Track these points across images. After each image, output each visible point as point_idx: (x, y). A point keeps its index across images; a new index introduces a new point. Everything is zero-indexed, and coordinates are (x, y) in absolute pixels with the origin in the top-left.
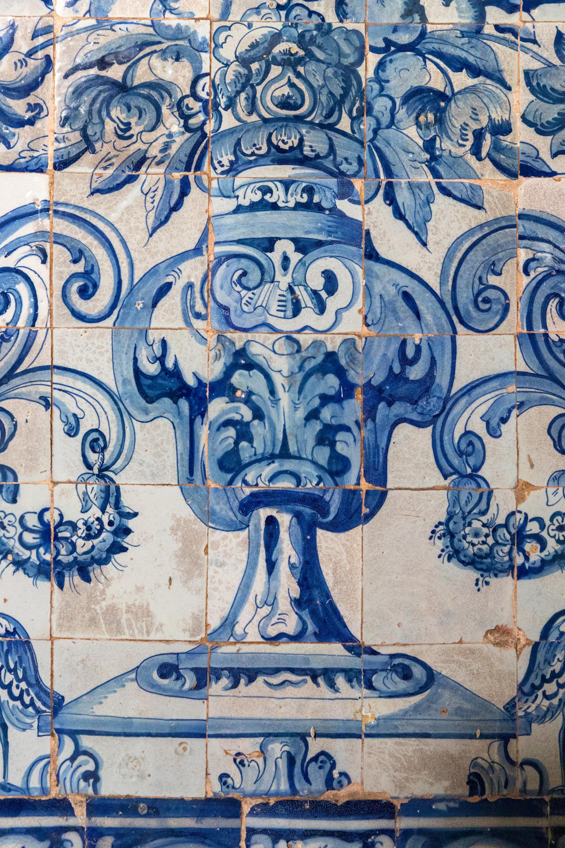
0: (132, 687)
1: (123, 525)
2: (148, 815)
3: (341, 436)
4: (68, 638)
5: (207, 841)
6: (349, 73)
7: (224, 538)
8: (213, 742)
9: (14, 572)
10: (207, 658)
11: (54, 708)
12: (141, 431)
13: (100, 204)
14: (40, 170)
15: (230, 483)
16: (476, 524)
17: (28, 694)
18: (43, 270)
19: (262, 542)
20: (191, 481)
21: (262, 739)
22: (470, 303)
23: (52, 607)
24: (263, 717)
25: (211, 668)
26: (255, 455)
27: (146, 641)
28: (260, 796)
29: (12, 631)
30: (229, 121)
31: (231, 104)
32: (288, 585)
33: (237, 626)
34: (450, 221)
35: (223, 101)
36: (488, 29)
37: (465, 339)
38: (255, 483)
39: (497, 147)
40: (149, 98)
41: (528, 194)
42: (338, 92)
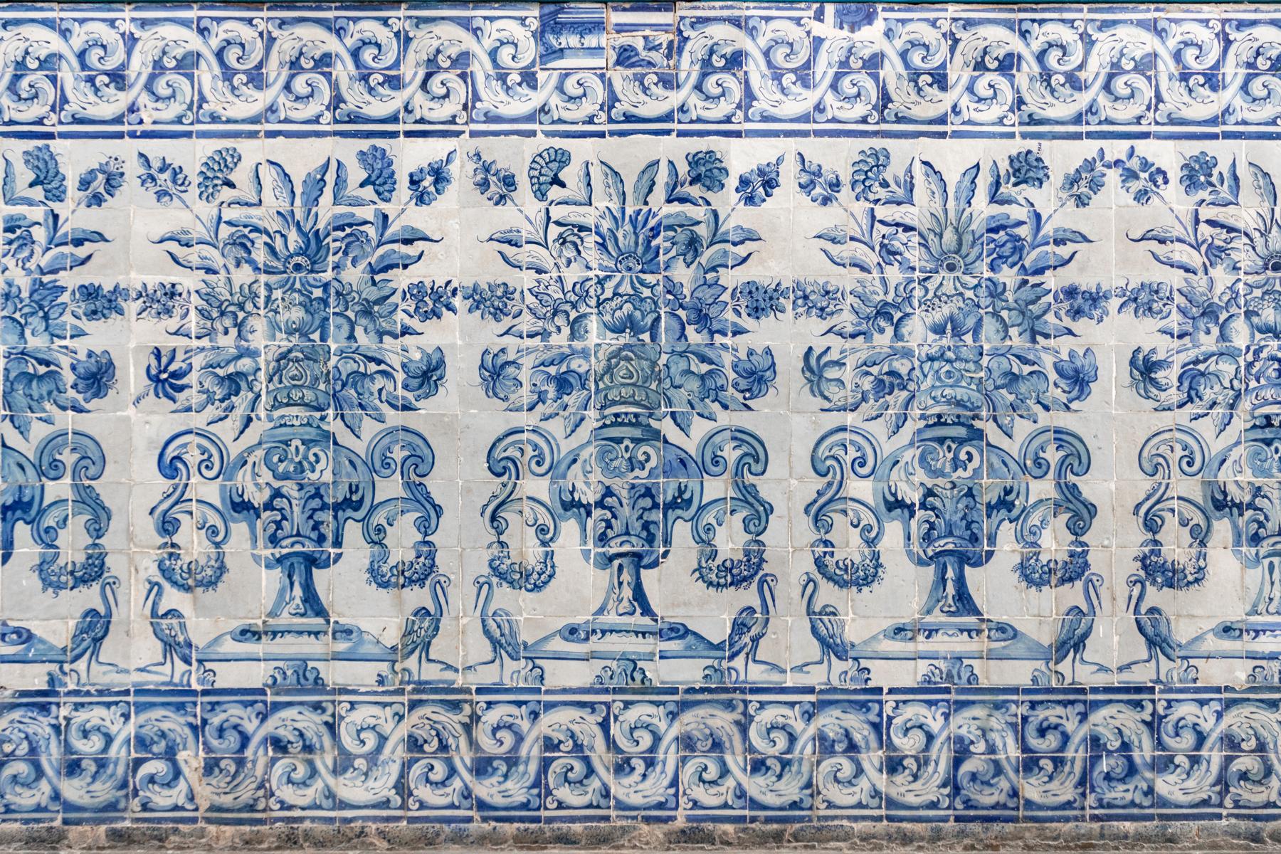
6: (654, 364)
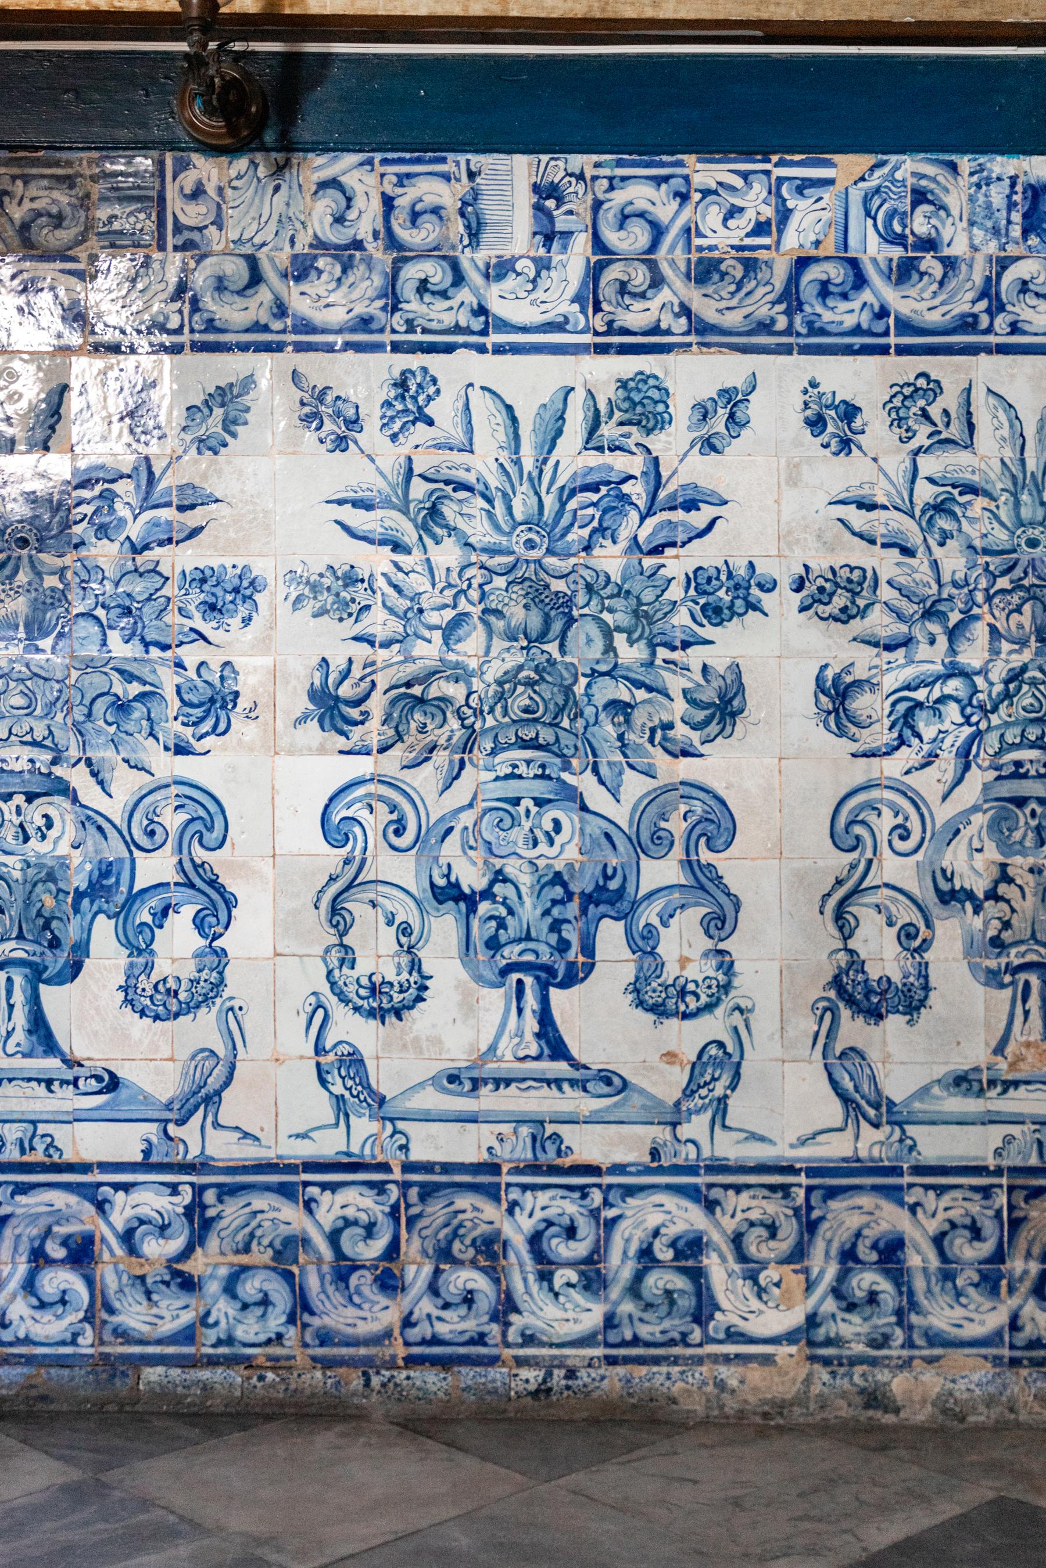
3: (565, 926)
6: (568, 691)
13: (408, 775)
14: (368, 754)
16: (654, 984)
18: (371, 818)
22: (649, 841)
30: (490, 722)
31: (491, 711)
32: (531, 1024)
34: (634, 786)
35: (486, 709)
36: (658, 662)
37: (645, 862)
39: (665, 738)
40: (438, 707)
41: (685, 769)
42: (561, 702)
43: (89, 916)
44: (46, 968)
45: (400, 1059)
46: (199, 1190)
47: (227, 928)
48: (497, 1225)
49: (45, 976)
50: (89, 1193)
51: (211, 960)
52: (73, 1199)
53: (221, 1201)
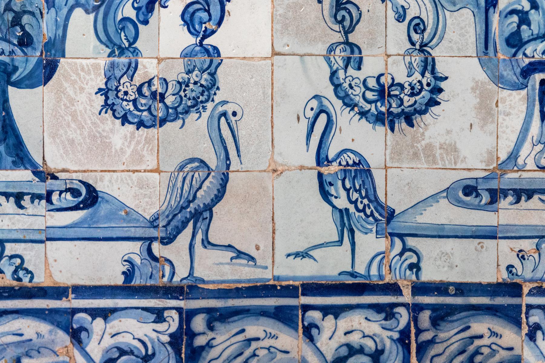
0: (444, 202)
1: (437, 86)
2: (455, 295)
4: (398, 168)
5: (498, 314)
7: (510, 95)
8: (502, 242)
9: (359, 120)
10: (497, 182)
11: (387, 217)
12: (450, 18)
15: (514, 55)
17: (369, 208)
19: (537, 98)
20: (486, 54)
21: (538, 240)
23: (386, 145)
24: (539, 224)
25: (500, 189)
26: (532, 35)
27: (454, 169)
28: (536, 281)
29: (358, 162)
33: (519, 158)
38: (532, 55)
43: (65, 10)
44: (16, 69)
45: (408, 170)
46: (187, 316)
47: (219, 24)
48: (517, 352)
49: (14, 78)
50: (63, 320)
51: (202, 60)
52: (44, 327)
53: (211, 328)
